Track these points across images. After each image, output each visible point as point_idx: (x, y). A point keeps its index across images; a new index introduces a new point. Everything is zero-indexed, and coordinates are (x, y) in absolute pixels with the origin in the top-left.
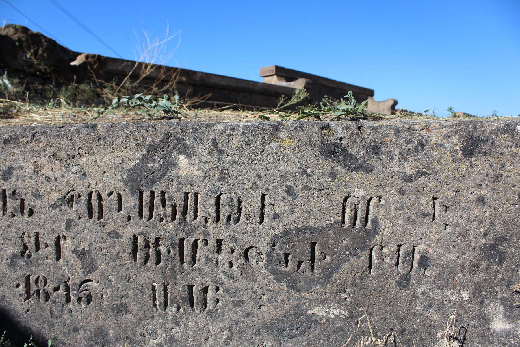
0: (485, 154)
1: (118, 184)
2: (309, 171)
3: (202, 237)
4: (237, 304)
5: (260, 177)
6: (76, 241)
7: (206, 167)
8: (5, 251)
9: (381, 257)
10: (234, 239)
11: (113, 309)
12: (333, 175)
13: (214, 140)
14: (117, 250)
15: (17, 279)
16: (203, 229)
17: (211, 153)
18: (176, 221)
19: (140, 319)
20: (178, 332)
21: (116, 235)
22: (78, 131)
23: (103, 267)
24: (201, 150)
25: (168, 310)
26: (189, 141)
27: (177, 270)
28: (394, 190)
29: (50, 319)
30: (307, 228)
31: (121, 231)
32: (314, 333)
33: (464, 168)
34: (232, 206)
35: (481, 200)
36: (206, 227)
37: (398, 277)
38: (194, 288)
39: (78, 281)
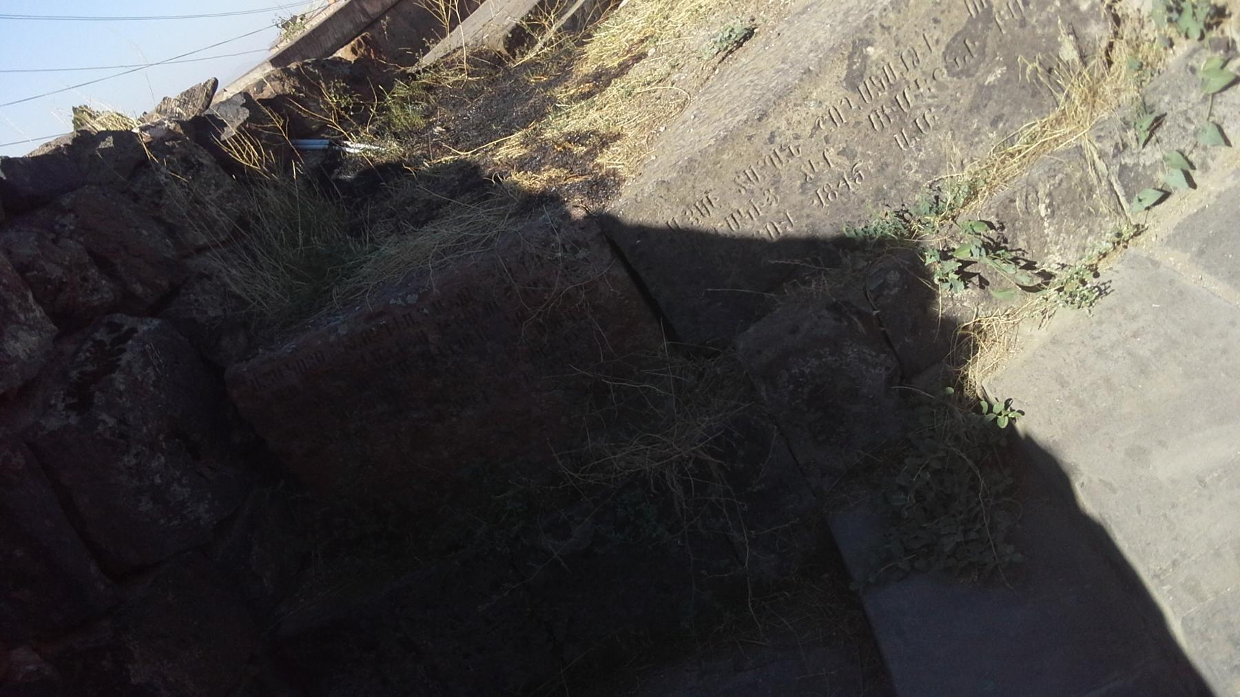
1: (843, 93)
4: (946, 111)
6: (835, 146)
8: (795, 186)
11: (878, 171)
14: (863, 132)
15: (811, 198)
16: (904, 81)
18: (886, 89)
19: (898, 164)
20: (922, 156)
21: (858, 123)
22: (801, 80)
23: (860, 149)
25: (910, 146)
29: (843, 207)
31: (860, 119)
36: (905, 79)
38: (917, 121)
39: (850, 170)
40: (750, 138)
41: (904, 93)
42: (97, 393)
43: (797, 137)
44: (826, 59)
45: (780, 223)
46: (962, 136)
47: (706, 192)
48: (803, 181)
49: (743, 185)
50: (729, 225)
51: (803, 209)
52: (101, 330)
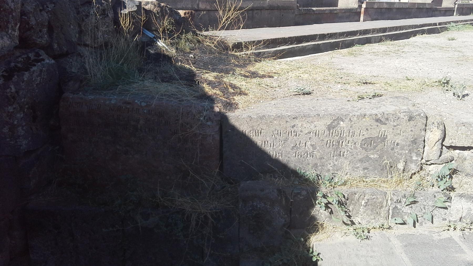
0: (413, 121)
2: (372, 125)
3: (345, 140)
4: (352, 155)
5: (360, 126)
7: (347, 124)
9: (387, 143)
10: (353, 140)
11: (320, 158)
12: (377, 126)
13: (350, 118)
17: (349, 121)
18: (339, 137)
20: (336, 163)
21: (323, 140)
22: (315, 116)
24: (347, 121)
26: (344, 119)
27: (338, 148)
28: (392, 129)
30: (371, 137)
31: (324, 139)
32: (370, 161)
33: (408, 124)
34: (353, 133)
35: (412, 131)
37: (391, 148)
38: (341, 152)
40: (287, 122)
41: (343, 142)
42: (16, 77)
43: (301, 131)
44: (327, 116)
45: (279, 154)
46: (352, 166)
47: (261, 129)
48: (294, 146)
49: (275, 134)
50: (262, 144)
51: (289, 154)
52: (33, 53)
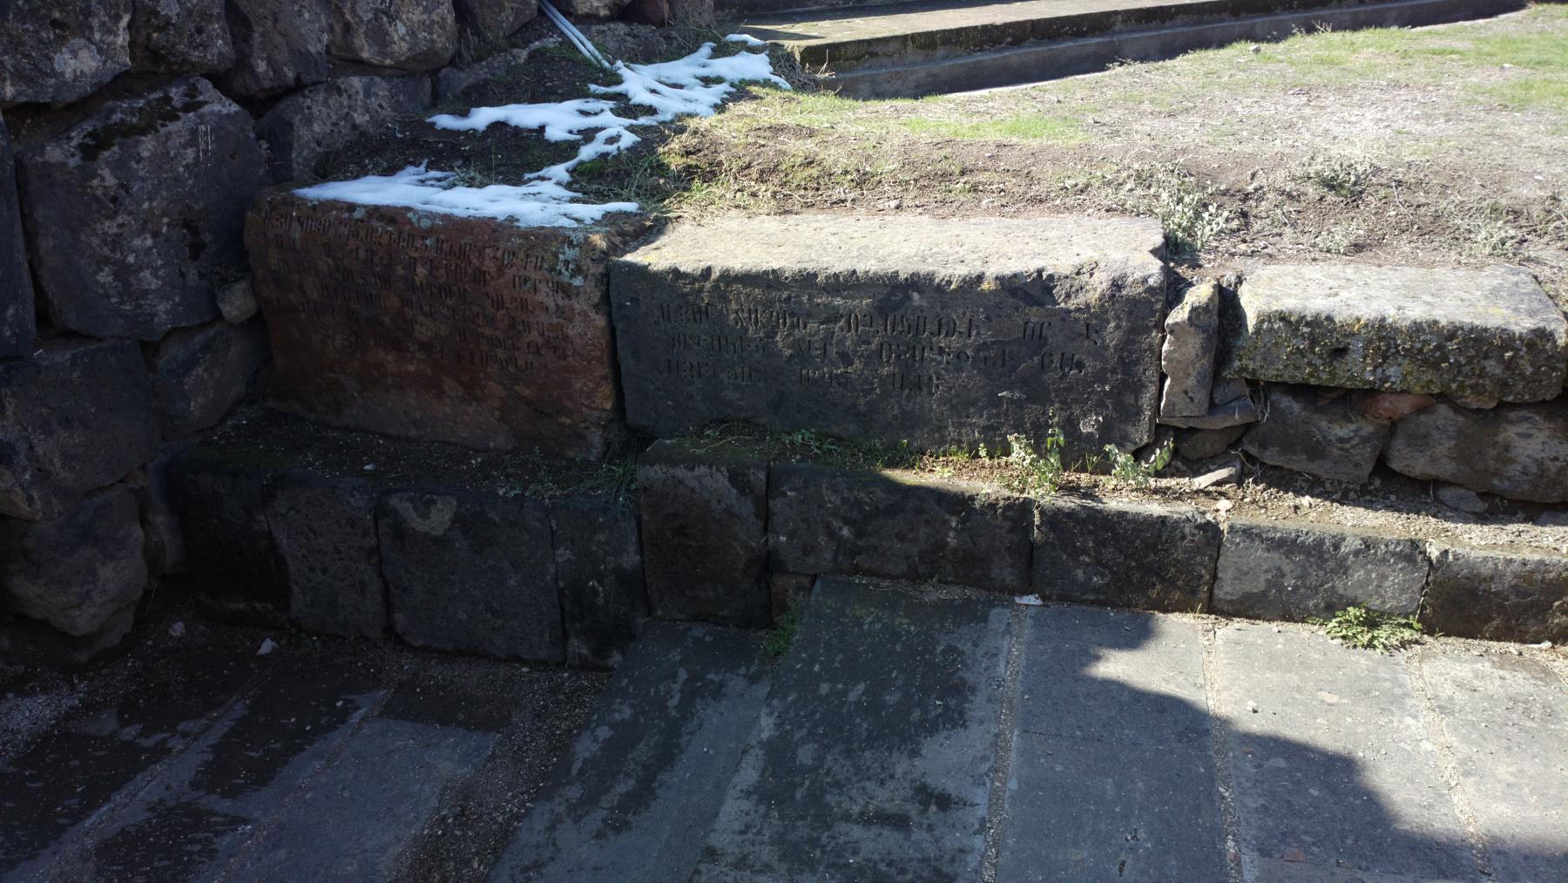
42: (116, 149)
52: (182, 88)
